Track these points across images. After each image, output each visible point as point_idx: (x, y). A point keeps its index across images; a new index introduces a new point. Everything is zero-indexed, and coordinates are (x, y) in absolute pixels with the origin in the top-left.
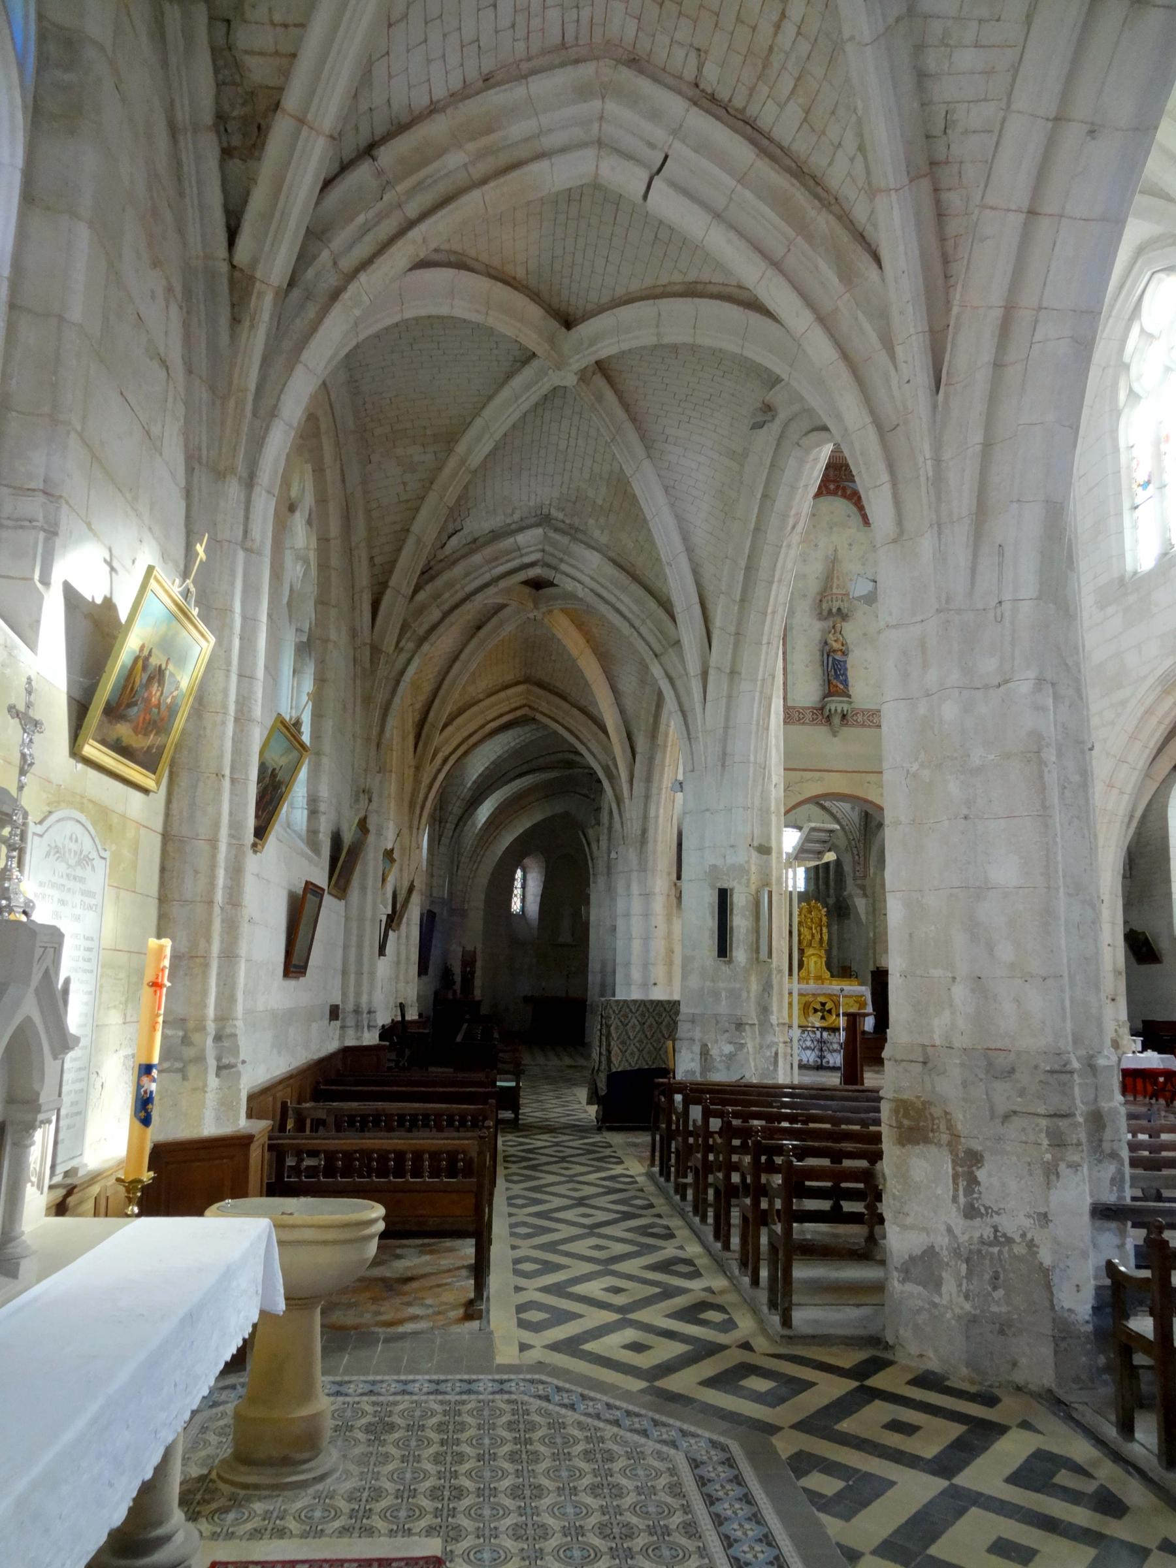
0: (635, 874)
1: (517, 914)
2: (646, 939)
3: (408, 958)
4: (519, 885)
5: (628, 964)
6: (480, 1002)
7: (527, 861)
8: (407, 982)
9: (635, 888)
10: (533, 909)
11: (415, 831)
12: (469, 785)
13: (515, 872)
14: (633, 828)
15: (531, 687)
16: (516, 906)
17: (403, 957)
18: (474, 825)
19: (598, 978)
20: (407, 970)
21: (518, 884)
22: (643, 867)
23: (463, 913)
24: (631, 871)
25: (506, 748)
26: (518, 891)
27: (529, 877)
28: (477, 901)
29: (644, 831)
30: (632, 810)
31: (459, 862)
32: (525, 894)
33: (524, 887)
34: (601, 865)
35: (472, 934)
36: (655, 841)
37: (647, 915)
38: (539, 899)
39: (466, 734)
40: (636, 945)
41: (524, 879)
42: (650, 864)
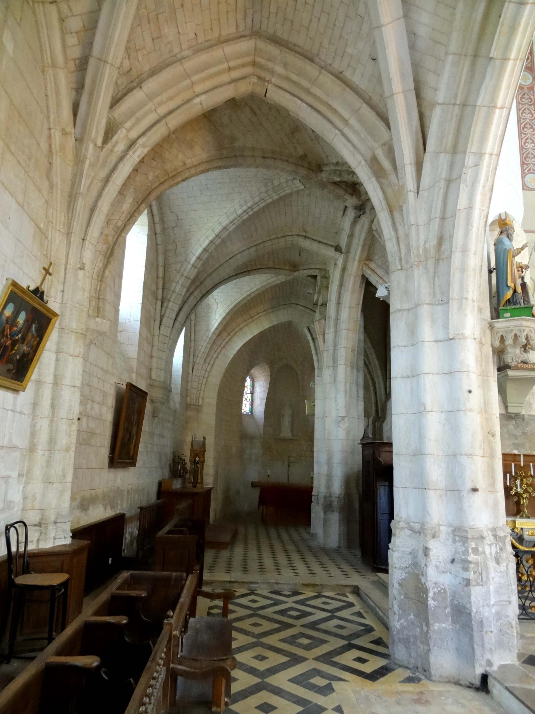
0: (425, 311)
1: (247, 415)
2: (453, 414)
3: (52, 441)
4: (249, 392)
5: (418, 454)
6: (208, 493)
7: (255, 371)
8: (48, 482)
9: (427, 332)
10: (260, 409)
11: (75, 240)
12: (192, 261)
13: (245, 380)
14: (422, 237)
15: (262, 45)
16: (246, 408)
17: (43, 437)
18: (208, 330)
19: (324, 469)
20: (48, 463)
21: (247, 390)
22: (443, 299)
23: (198, 408)
24: (417, 306)
25: (231, 218)
26: (247, 396)
27: (257, 385)
28: (210, 400)
29: (442, 240)
30: (418, 212)
31: (194, 363)
32: (254, 396)
33: (252, 393)
34: (327, 358)
35: (205, 427)
36: (465, 251)
37: (451, 373)
38: (264, 402)
39: (162, 110)
40: (434, 425)
41: (253, 387)
42: (454, 292)
